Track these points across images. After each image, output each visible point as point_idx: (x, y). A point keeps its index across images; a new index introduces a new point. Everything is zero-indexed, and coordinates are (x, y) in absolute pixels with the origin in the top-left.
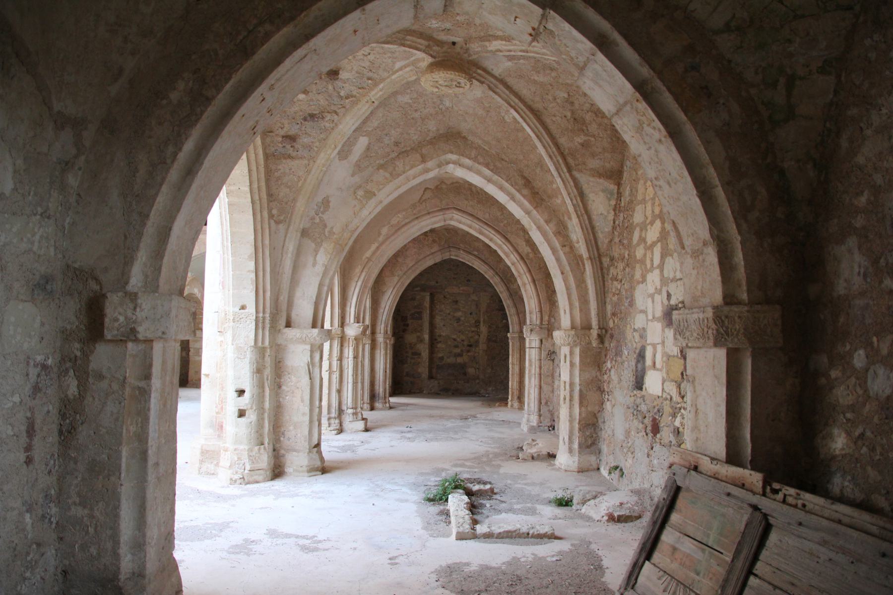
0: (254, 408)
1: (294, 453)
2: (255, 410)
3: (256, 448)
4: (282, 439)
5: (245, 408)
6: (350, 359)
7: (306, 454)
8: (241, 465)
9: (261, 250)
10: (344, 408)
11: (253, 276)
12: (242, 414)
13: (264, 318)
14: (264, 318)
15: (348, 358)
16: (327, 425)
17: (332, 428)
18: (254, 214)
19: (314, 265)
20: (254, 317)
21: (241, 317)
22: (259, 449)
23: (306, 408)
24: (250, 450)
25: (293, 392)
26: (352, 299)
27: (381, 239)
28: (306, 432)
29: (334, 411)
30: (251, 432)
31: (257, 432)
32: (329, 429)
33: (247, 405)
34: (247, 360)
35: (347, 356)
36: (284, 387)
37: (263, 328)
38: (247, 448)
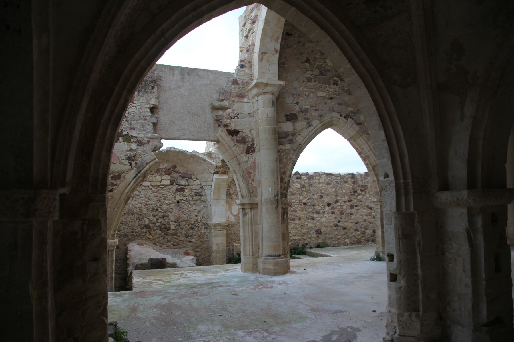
0: (403, 274)
1: (459, 327)
2: (404, 276)
3: (407, 314)
4: (448, 308)
5: (394, 272)
8: (393, 328)
9: (388, 118)
11: (386, 144)
12: (393, 278)
13: (406, 184)
14: (406, 184)
18: (367, 86)
20: (394, 185)
22: (410, 316)
23: (468, 279)
28: (470, 306)
30: (400, 297)
34: (393, 226)
36: (447, 254)
37: (407, 194)
38: (397, 312)
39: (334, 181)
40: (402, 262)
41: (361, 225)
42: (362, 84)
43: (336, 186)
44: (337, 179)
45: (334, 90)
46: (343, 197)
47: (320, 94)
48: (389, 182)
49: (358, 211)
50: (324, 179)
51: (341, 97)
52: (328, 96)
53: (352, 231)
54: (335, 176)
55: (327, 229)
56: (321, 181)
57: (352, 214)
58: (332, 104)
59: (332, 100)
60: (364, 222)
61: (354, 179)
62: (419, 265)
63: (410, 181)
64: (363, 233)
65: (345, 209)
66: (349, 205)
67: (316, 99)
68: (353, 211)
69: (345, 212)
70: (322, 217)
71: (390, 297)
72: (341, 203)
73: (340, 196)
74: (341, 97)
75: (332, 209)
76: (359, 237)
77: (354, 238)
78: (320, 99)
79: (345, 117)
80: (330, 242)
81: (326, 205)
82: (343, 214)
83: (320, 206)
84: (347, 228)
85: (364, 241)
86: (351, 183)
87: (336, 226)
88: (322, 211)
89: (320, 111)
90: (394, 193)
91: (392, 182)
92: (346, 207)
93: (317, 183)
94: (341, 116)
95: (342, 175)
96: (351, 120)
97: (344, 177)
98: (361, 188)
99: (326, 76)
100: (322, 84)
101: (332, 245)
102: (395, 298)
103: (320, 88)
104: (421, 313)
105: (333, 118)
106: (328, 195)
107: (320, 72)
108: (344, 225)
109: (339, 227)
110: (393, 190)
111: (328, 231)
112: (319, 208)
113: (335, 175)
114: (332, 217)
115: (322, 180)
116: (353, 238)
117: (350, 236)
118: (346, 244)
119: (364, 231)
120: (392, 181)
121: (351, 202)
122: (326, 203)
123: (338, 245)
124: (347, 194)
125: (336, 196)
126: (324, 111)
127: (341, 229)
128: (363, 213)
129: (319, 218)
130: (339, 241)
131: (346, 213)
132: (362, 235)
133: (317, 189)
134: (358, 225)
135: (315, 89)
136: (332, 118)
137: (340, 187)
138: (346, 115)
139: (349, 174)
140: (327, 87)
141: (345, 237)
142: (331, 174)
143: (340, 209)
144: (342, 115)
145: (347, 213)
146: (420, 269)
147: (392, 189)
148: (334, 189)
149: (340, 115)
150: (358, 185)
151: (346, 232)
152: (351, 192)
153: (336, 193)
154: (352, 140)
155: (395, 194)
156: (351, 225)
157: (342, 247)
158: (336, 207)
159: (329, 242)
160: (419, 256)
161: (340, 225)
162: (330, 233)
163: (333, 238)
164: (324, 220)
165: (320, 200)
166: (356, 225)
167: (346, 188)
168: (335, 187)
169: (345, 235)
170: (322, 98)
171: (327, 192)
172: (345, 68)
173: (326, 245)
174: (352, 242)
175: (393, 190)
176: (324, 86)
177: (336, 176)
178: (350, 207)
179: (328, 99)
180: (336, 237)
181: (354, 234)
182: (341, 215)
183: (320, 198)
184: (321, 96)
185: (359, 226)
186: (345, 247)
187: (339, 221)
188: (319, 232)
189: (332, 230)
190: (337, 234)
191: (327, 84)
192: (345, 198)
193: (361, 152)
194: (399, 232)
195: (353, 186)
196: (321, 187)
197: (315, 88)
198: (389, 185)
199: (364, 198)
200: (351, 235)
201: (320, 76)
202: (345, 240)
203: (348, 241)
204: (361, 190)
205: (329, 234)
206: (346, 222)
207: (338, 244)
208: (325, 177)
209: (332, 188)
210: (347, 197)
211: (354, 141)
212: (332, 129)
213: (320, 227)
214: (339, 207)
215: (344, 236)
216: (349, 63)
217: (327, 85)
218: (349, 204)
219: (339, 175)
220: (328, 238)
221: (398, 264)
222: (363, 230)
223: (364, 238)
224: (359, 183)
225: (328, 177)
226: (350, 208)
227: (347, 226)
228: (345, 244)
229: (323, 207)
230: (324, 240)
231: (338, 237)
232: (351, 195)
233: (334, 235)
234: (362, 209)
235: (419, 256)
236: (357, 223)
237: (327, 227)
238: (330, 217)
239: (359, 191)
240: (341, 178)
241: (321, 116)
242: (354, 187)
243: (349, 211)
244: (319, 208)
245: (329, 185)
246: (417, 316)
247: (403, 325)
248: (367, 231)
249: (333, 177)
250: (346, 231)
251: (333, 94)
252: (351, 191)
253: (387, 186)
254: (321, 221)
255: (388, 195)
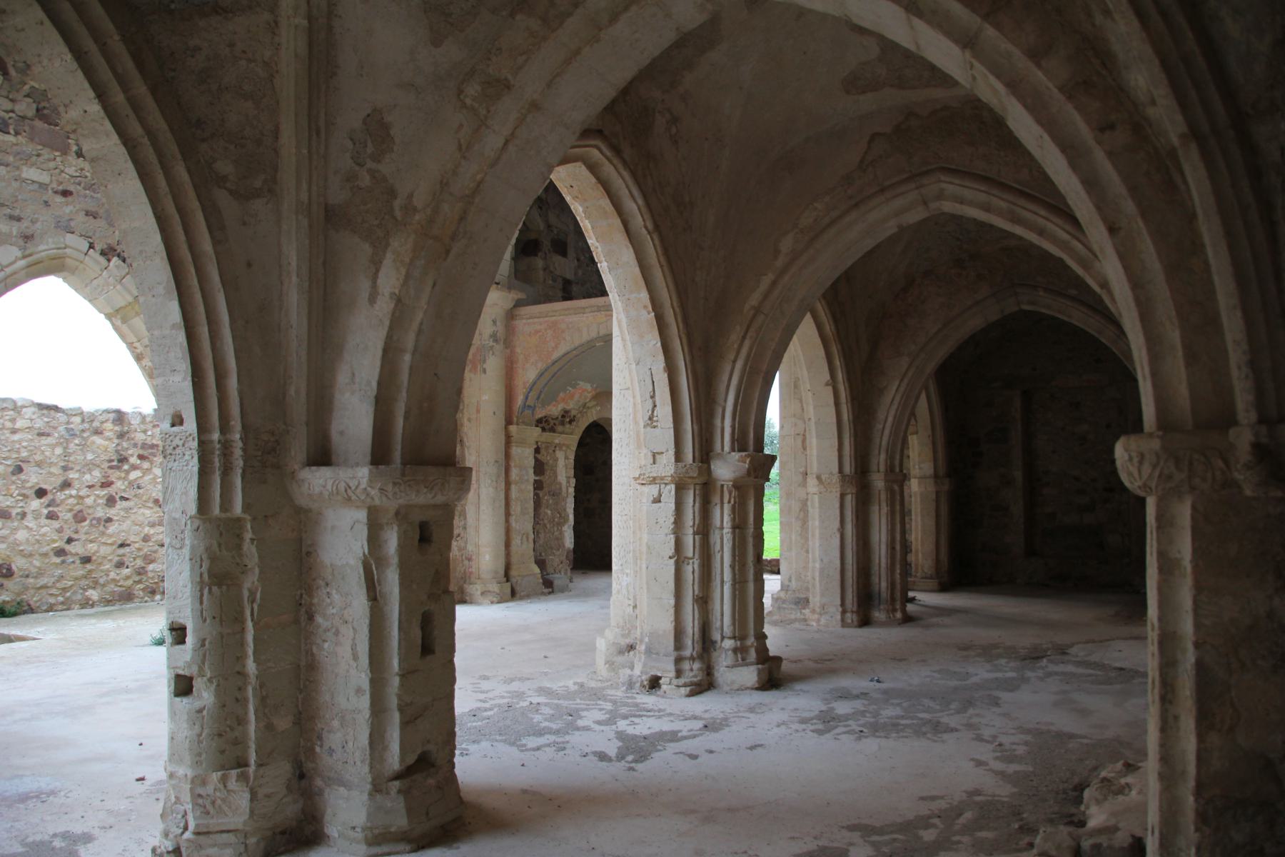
0: (209, 675)
1: (342, 789)
2: (210, 680)
3: (215, 776)
4: (318, 749)
5: (186, 673)
6: (725, 531)
7: (365, 797)
8: (180, 816)
9: (192, 270)
10: (716, 636)
11: (181, 337)
12: (183, 686)
13: (226, 446)
14: (226, 446)
15: (722, 528)
16: (673, 674)
17: (682, 681)
19: (372, 299)
21: (174, 444)
22: (224, 780)
23: (363, 675)
24: (199, 781)
25: (337, 633)
26: (725, 401)
27: (779, 263)
29: (689, 642)
30: (200, 735)
31: (220, 735)
32: (675, 682)
33: (189, 665)
34: (186, 551)
35: (718, 523)
36: (319, 619)
37: (227, 471)
38: (190, 773)
39: (61, 429)
40: (207, 643)
41: (134, 549)
42: (130, 165)
43: (67, 441)
44: (72, 423)
45: (76, 171)
46: (84, 473)
47: (31, 173)
48: (184, 437)
49: (127, 512)
50: (31, 420)
51: (95, 195)
52: (59, 186)
53: (108, 566)
54: (67, 414)
55: (31, 563)
56: (19, 424)
57: (109, 520)
58: (68, 210)
59: (70, 199)
60: (144, 543)
61: (123, 427)
62: (250, 651)
63: (238, 436)
64: (141, 572)
65: (89, 507)
66: (104, 496)
67: (15, 185)
68: (112, 512)
69: (89, 514)
70: (16, 529)
71: (172, 738)
72: (78, 490)
73: (77, 471)
74: (95, 195)
75: (49, 505)
76: (129, 582)
77: (112, 586)
78: (31, 187)
79: (103, 253)
80: (40, 600)
81: (31, 493)
82: (84, 520)
83: (11, 496)
84: (94, 558)
85: (141, 593)
86: (112, 436)
87: (60, 552)
88: (19, 510)
89: (25, 224)
90: (194, 465)
91: (191, 438)
92: (94, 502)
93: (7, 429)
94: (91, 246)
95: (88, 413)
96: (122, 263)
97: (92, 418)
98: (141, 452)
99: (58, 128)
100: (40, 147)
101: (45, 608)
102: (186, 737)
103: (35, 158)
104: (252, 769)
105: (67, 250)
106: (39, 464)
107: (38, 110)
108: (86, 550)
109: (69, 556)
110: (192, 457)
111: (35, 567)
112: (8, 503)
113: (67, 410)
114: (48, 528)
115: (24, 421)
116: (112, 587)
117: (102, 581)
118: (87, 603)
119: (143, 568)
120: (190, 435)
121: (109, 489)
122: (31, 488)
123: (65, 607)
124: (99, 466)
125: (65, 469)
126: (39, 223)
127: (73, 562)
128: (141, 518)
129: (8, 532)
130: (68, 594)
131: (91, 517)
132: (137, 578)
133: (6, 447)
134: (127, 549)
135: (15, 156)
136: (65, 248)
137: (77, 445)
138: (105, 246)
139: (107, 411)
140: (55, 159)
141: (87, 585)
142: (56, 409)
143: (75, 505)
144: (96, 245)
145: (94, 518)
146: (252, 658)
147: (189, 455)
148: (59, 451)
149: (88, 245)
150: (133, 442)
151: (90, 571)
152: (113, 461)
153: (65, 460)
154: (118, 317)
155: (196, 469)
156: (104, 550)
157: (76, 611)
158: (65, 499)
159: (35, 599)
160: (249, 625)
161: (73, 551)
162: (41, 574)
163: (48, 587)
164: (21, 535)
165: (14, 478)
166: (122, 551)
167: (98, 448)
168: (64, 443)
169: (86, 577)
170: (36, 186)
171: (38, 457)
172: (86, 112)
173: (26, 608)
174: (107, 597)
175: (192, 457)
176: (46, 153)
177: (71, 412)
178: (105, 502)
179: (56, 192)
180: (58, 585)
181: (112, 575)
182: (76, 522)
183: (13, 473)
184: (35, 179)
185: (129, 552)
186: (83, 611)
187: (70, 541)
188: (4, 571)
189: (47, 564)
190: (62, 577)
191: (57, 150)
192: (92, 475)
193: (142, 354)
194: (201, 566)
195: (118, 445)
196: (20, 442)
197: (19, 153)
198: (183, 445)
199: (147, 478)
200: (105, 578)
201: (39, 124)
202: (87, 594)
203: (94, 594)
204: (141, 457)
205: (36, 577)
206: (91, 541)
207: (62, 603)
208: (34, 413)
209: (53, 447)
210: (97, 473)
211: (124, 321)
212: (61, 279)
213: (8, 556)
214: (71, 501)
215: (84, 583)
216: (97, 101)
217: (57, 154)
218: (104, 493)
219: (80, 413)
220: (33, 588)
221: (195, 650)
222: (139, 563)
223: (141, 586)
224: (137, 438)
225: (43, 414)
226: (106, 505)
227: (94, 554)
228: (87, 604)
229: (21, 498)
230: (18, 594)
231: (66, 584)
232: (111, 468)
233: (53, 580)
234: (140, 508)
235: (249, 625)
236: (122, 545)
237: (31, 555)
238: (43, 527)
239: (134, 460)
240: (83, 421)
241: (27, 238)
242: (119, 448)
243: (100, 513)
244: (7, 500)
245: (44, 438)
246: (243, 777)
247: (205, 807)
248: (151, 567)
249: (60, 414)
250: (89, 566)
251: (72, 181)
252: (112, 458)
253: (178, 446)
254: (11, 539)
255: (179, 470)
